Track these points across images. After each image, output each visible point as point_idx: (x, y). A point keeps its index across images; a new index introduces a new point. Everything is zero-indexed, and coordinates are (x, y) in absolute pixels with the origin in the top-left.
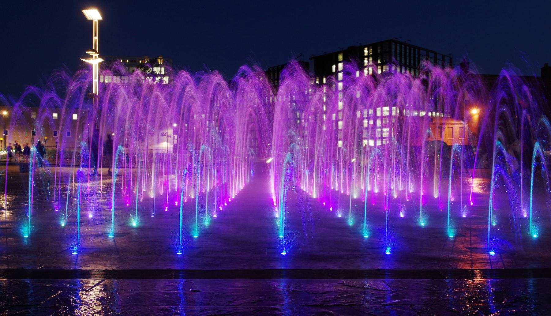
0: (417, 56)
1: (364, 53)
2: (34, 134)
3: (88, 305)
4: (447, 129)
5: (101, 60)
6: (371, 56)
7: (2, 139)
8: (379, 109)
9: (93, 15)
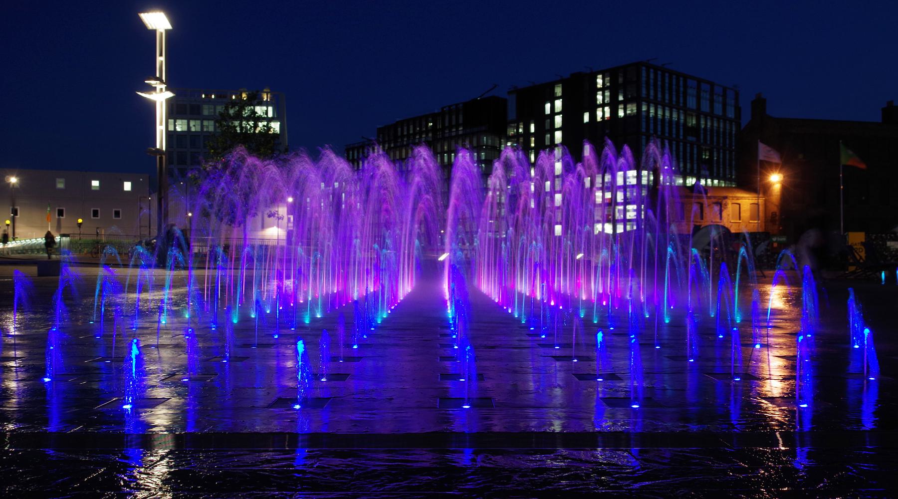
0: (682, 89)
1: (596, 83)
2: (61, 213)
3: (149, 490)
4: (730, 206)
5: (170, 95)
6: (607, 88)
7: (8, 222)
8: (620, 174)
9: (157, 21)
